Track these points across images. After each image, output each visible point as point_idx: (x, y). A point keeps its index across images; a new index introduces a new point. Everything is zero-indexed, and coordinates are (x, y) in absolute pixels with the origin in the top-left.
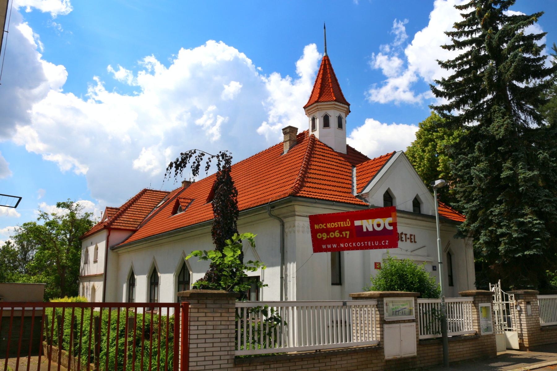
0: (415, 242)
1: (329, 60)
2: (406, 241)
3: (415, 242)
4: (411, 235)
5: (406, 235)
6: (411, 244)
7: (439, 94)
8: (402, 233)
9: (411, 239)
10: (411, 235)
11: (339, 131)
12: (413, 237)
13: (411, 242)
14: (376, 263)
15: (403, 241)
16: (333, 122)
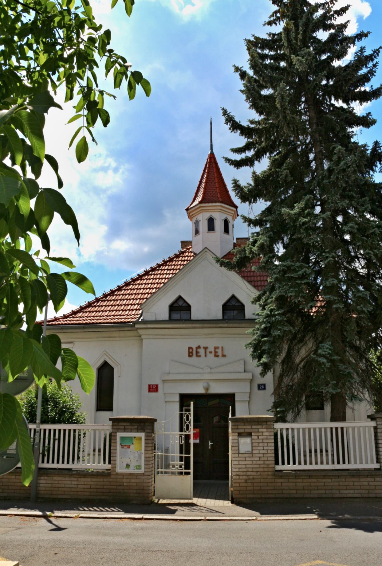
0: (224, 356)
1: (214, 158)
2: (206, 356)
3: (224, 356)
4: (216, 348)
5: (206, 348)
6: (216, 358)
7: (248, 162)
8: (199, 347)
9: (216, 352)
10: (216, 348)
11: (226, 236)
12: (219, 352)
13: (216, 356)
14: (149, 386)
15: (200, 356)
16: (219, 225)
